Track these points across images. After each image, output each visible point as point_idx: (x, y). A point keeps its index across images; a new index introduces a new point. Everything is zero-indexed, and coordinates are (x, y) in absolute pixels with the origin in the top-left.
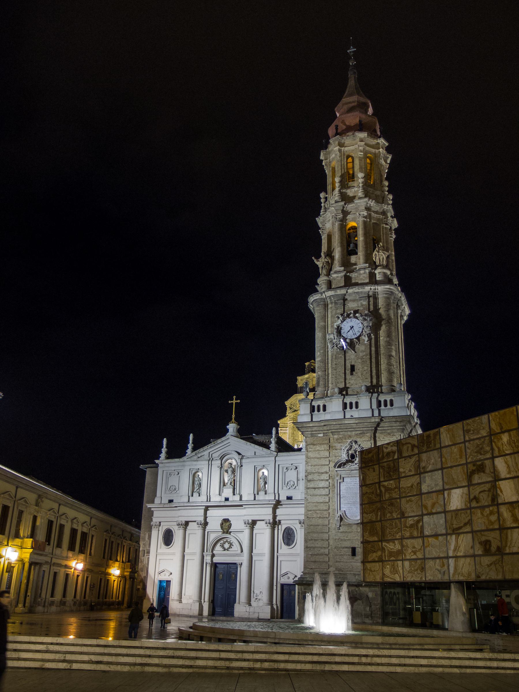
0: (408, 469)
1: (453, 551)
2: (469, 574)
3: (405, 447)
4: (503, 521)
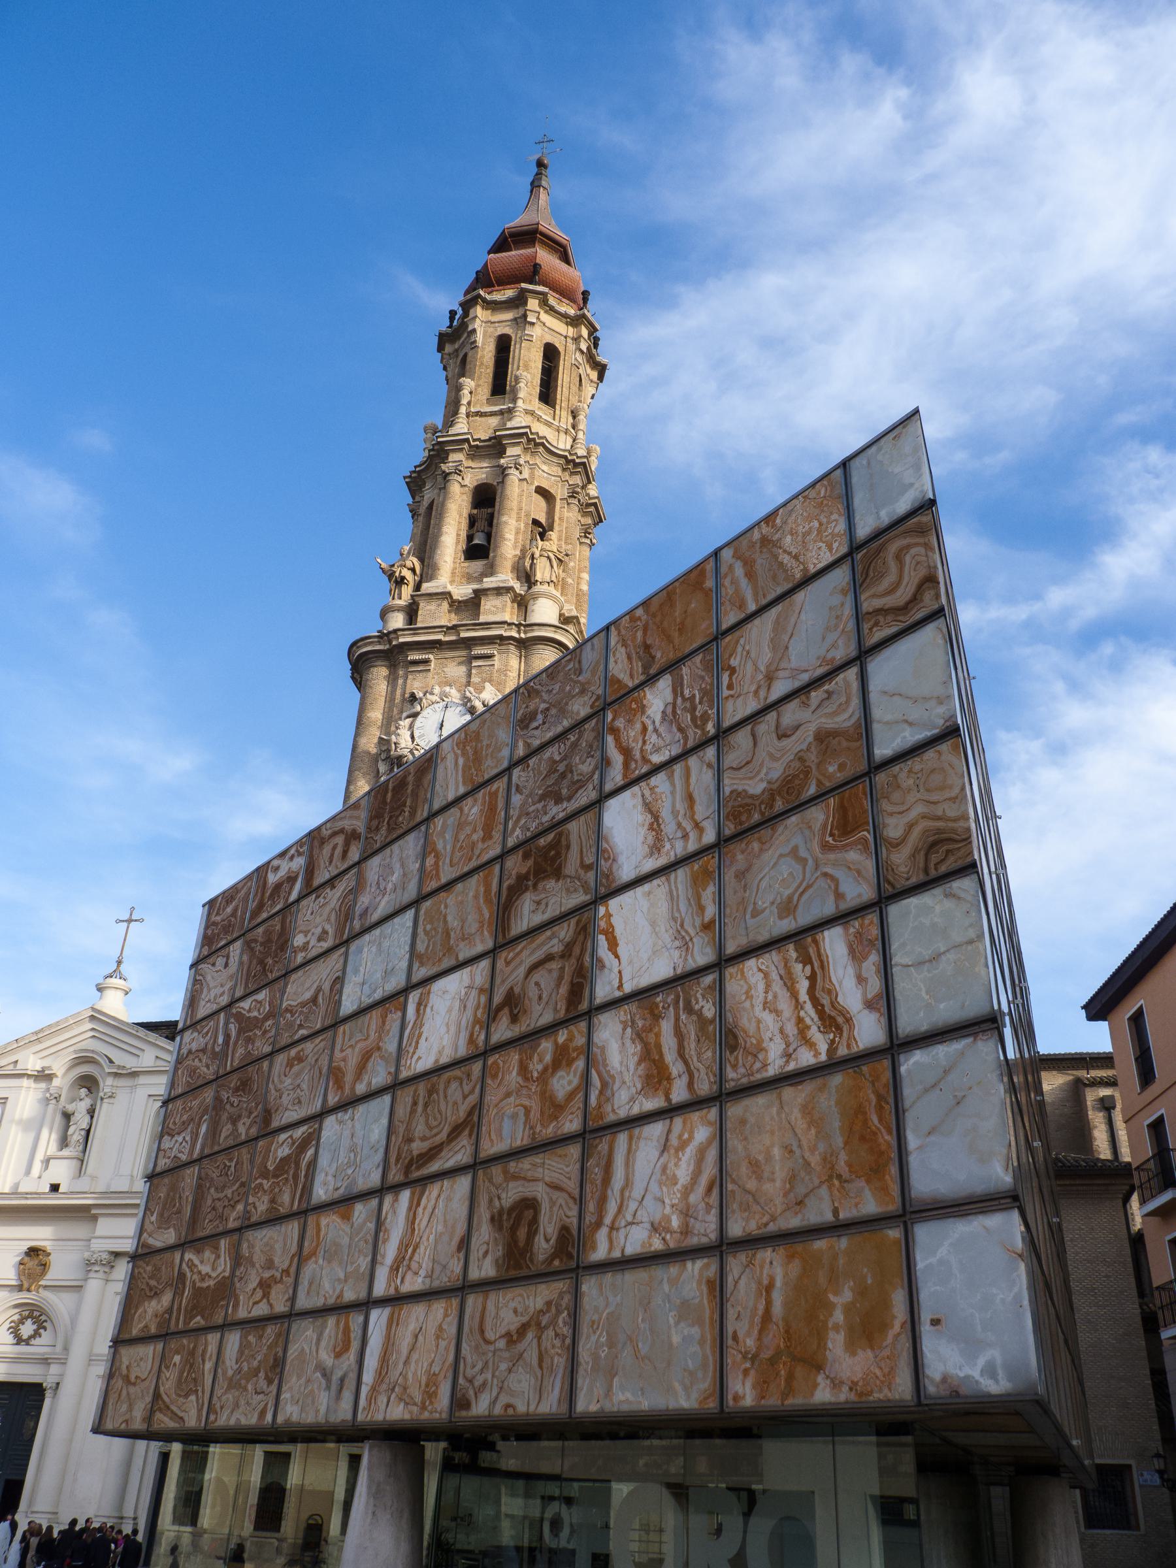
0: (319, 930)
1: (391, 1267)
2: (430, 1394)
3: (327, 850)
4: (601, 1093)
